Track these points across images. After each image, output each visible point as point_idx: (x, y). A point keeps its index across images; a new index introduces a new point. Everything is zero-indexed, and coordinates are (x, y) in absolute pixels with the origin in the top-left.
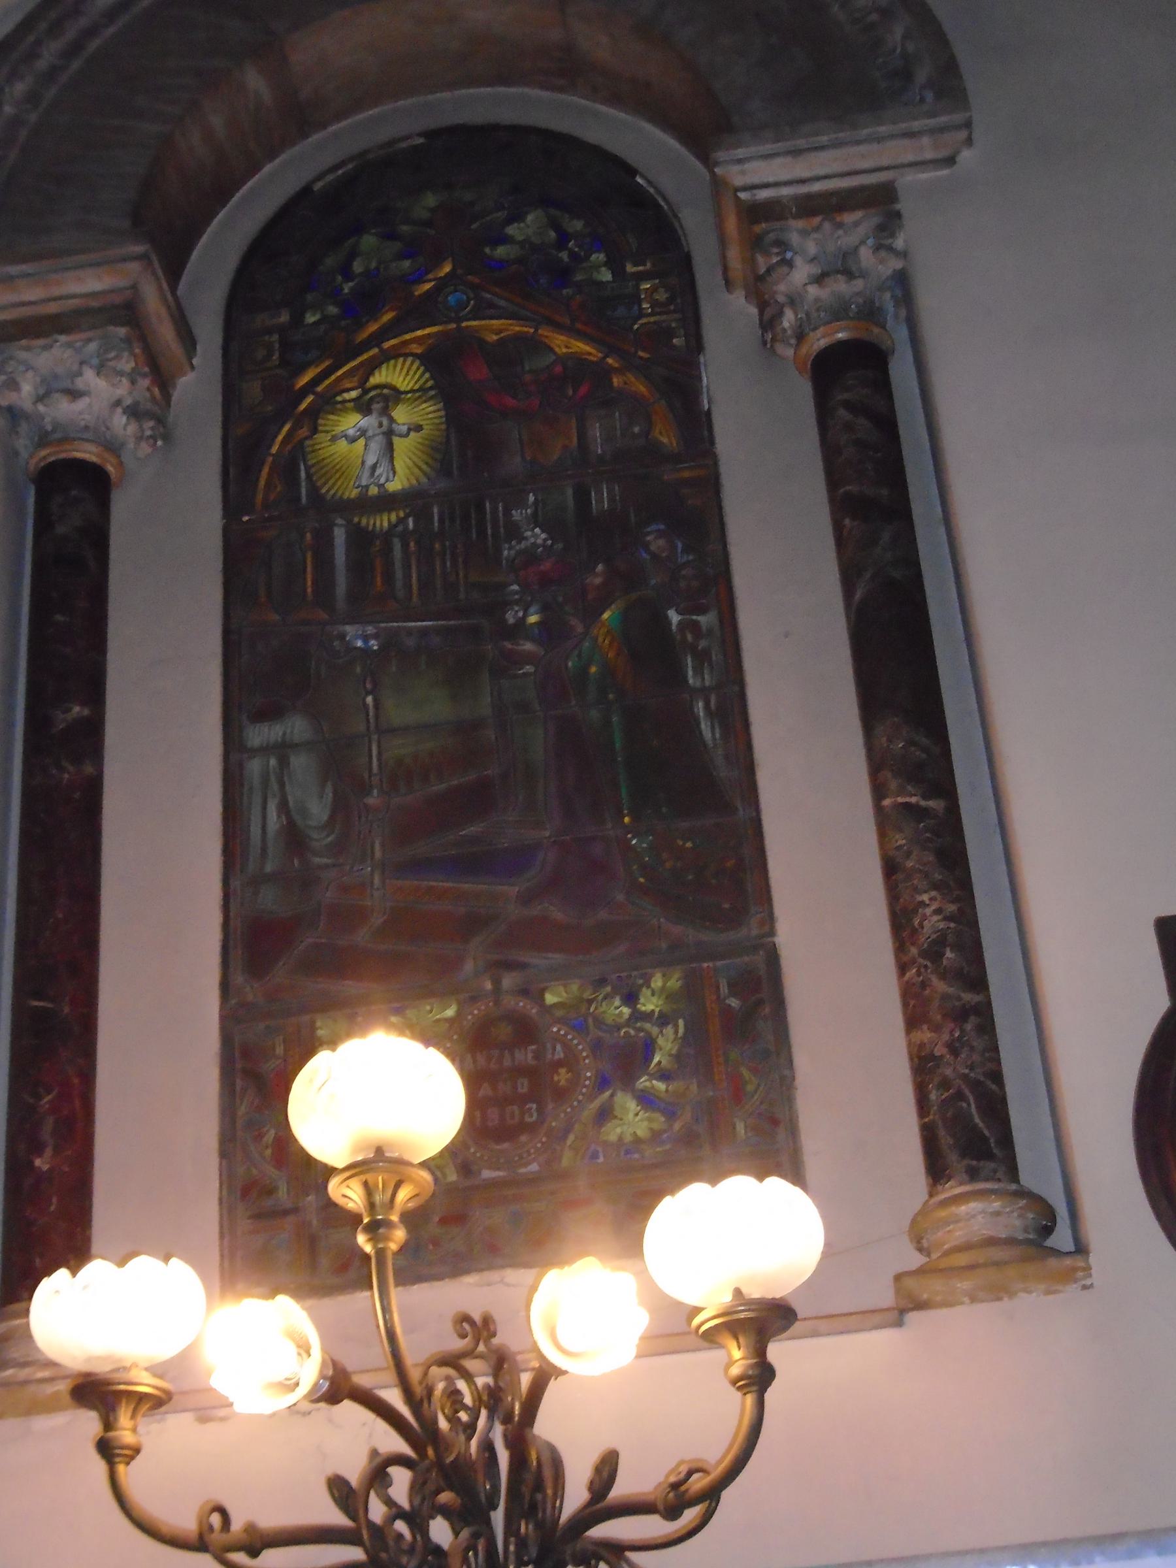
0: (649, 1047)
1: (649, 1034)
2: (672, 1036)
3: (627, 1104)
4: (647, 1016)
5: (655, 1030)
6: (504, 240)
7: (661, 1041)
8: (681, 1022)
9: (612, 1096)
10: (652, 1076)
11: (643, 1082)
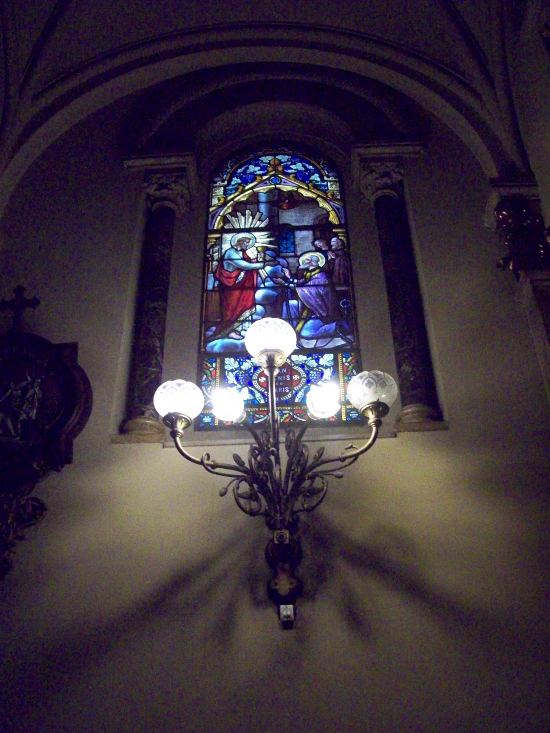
1: (322, 370)
4: (322, 366)
5: (324, 370)
6: (292, 169)
8: (332, 368)
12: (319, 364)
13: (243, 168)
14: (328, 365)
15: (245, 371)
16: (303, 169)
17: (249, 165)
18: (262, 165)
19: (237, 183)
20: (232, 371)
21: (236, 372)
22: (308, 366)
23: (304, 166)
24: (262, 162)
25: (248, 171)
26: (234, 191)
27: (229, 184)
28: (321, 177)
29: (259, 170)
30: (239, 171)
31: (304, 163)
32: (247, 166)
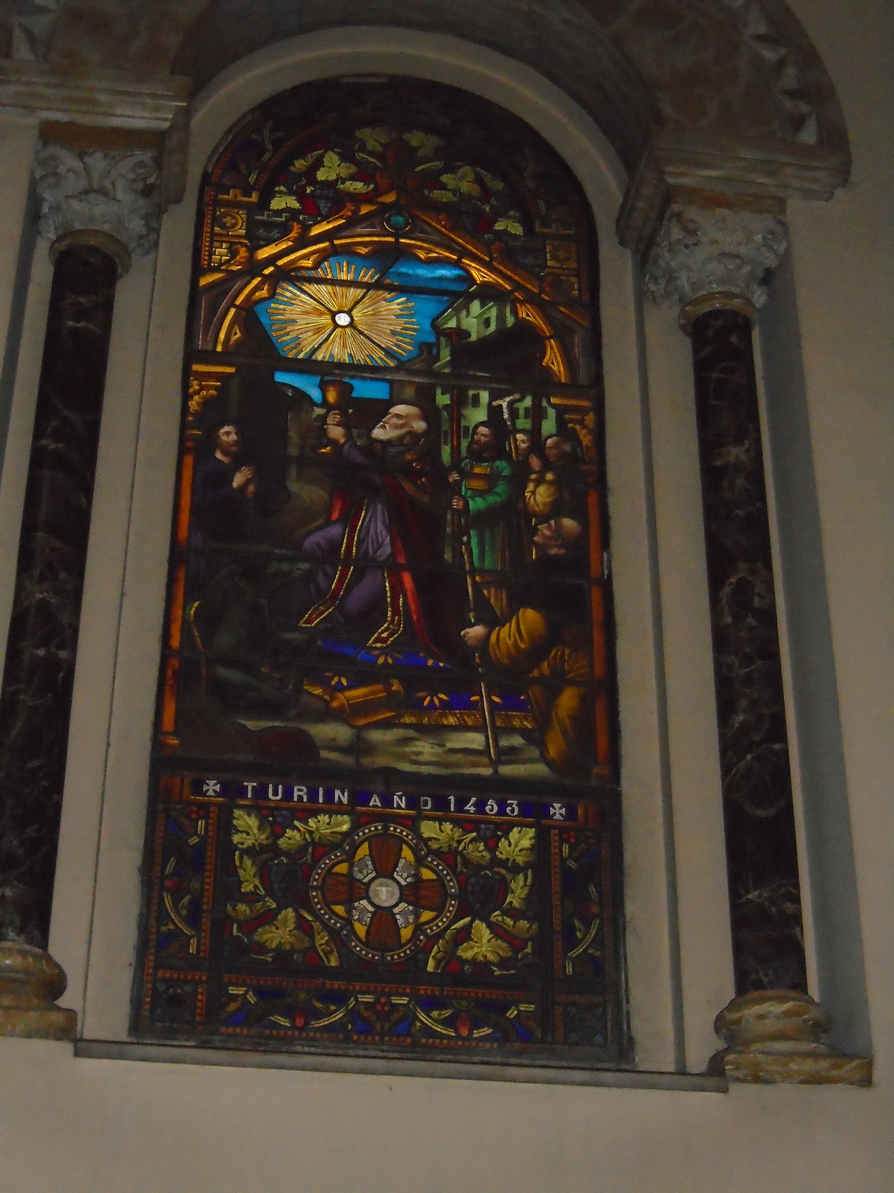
0: (505, 890)
1: (503, 878)
2: (521, 883)
3: (482, 930)
4: (503, 863)
5: (509, 876)
7: (513, 885)
9: (472, 922)
10: (505, 913)
11: (496, 916)
12: (494, 858)
13: (310, 159)
14: (520, 860)
15: (287, 854)
16: (476, 191)
17: (325, 152)
19: (287, 210)
20: (250, 852)
21: (264, 856)
22: (466, 861)
23: (479, 180)
24: (363, 148)
25: (321, 175)
26: (275, 234)
28: (527, 221)
30: (300, 164)
31: (478, 169)
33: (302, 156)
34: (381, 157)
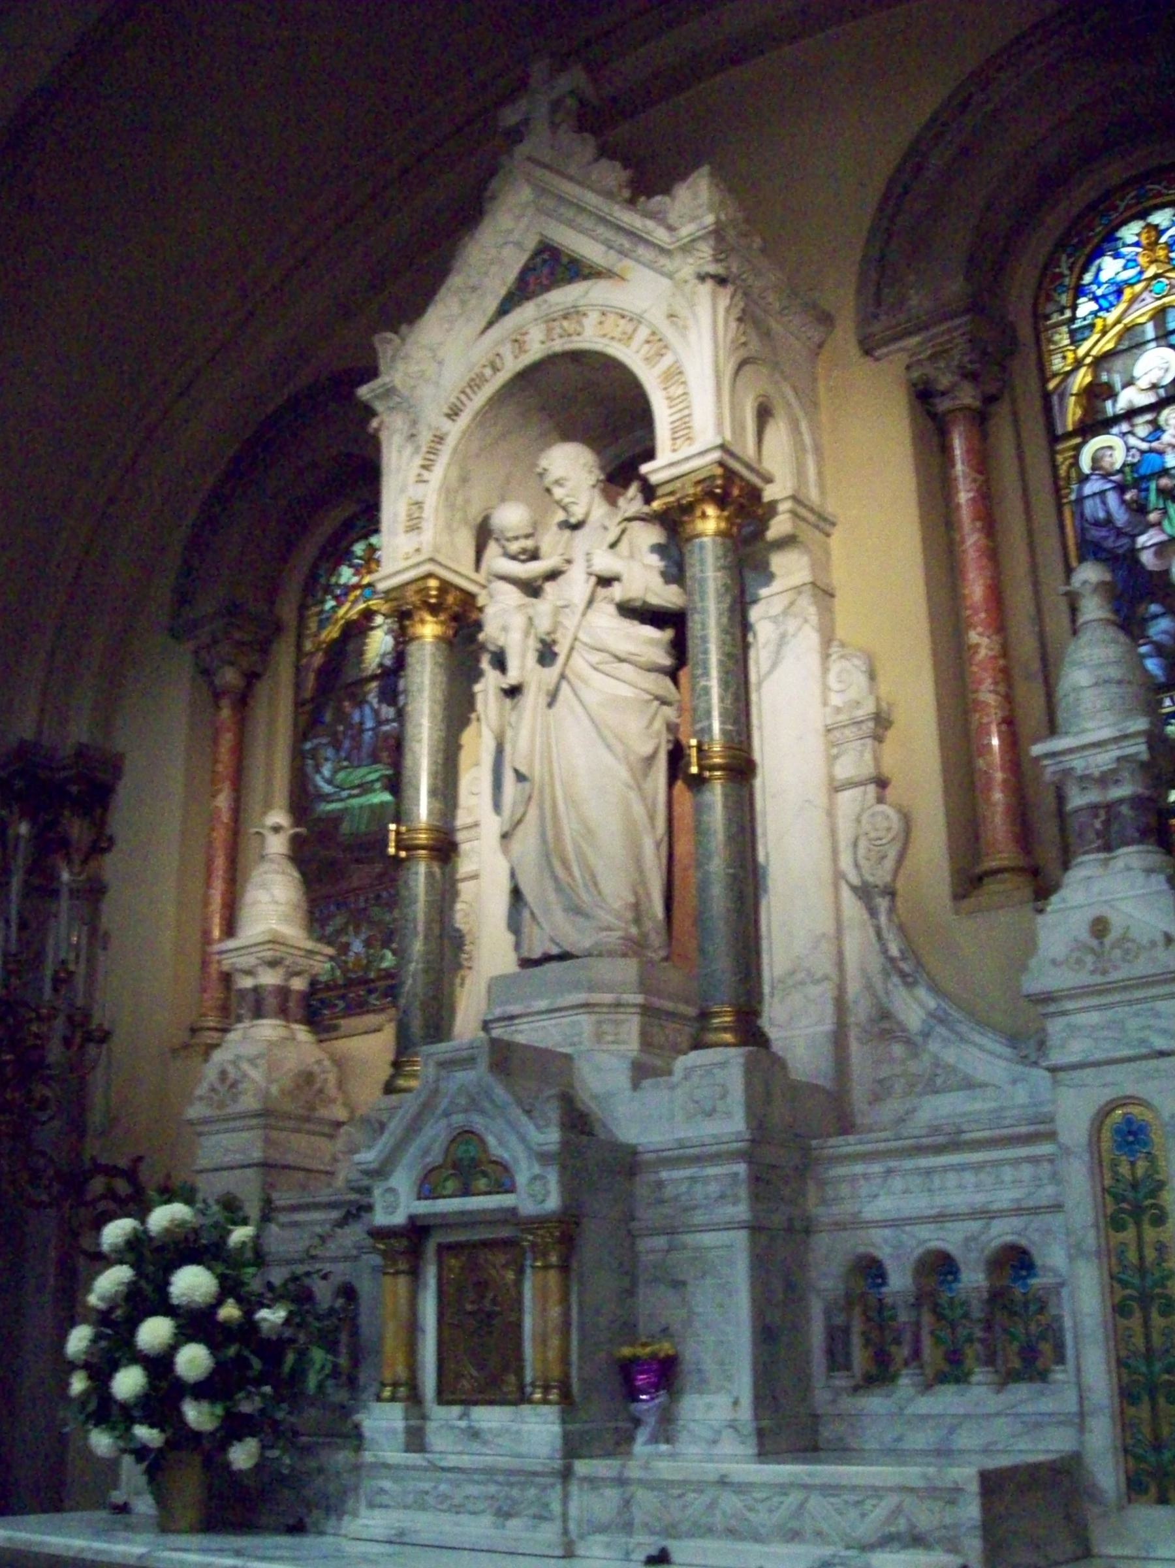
13: (1093, 269)
18: (1124, 250)
25: (1104, 277)
27: (1073, 319)
29: (1125, 268)
30: (1088, 278)
32: (1097, 262)
33: (1085, 269)
34: (1137, 244)
